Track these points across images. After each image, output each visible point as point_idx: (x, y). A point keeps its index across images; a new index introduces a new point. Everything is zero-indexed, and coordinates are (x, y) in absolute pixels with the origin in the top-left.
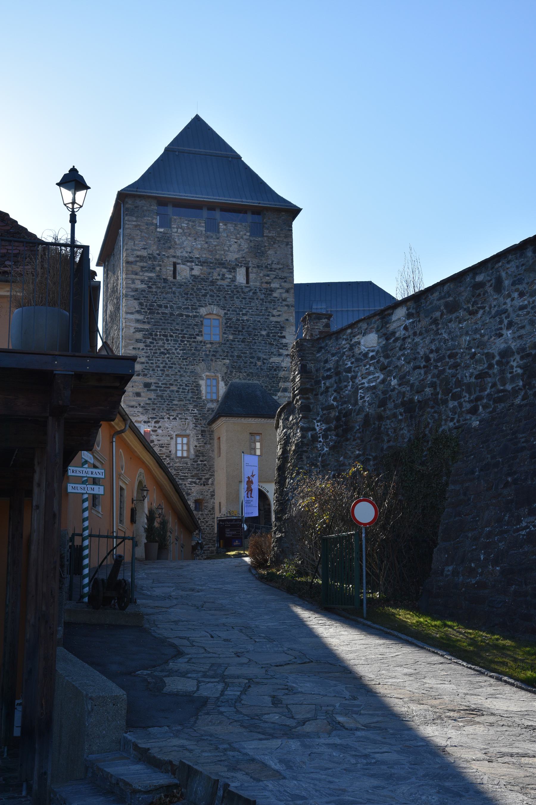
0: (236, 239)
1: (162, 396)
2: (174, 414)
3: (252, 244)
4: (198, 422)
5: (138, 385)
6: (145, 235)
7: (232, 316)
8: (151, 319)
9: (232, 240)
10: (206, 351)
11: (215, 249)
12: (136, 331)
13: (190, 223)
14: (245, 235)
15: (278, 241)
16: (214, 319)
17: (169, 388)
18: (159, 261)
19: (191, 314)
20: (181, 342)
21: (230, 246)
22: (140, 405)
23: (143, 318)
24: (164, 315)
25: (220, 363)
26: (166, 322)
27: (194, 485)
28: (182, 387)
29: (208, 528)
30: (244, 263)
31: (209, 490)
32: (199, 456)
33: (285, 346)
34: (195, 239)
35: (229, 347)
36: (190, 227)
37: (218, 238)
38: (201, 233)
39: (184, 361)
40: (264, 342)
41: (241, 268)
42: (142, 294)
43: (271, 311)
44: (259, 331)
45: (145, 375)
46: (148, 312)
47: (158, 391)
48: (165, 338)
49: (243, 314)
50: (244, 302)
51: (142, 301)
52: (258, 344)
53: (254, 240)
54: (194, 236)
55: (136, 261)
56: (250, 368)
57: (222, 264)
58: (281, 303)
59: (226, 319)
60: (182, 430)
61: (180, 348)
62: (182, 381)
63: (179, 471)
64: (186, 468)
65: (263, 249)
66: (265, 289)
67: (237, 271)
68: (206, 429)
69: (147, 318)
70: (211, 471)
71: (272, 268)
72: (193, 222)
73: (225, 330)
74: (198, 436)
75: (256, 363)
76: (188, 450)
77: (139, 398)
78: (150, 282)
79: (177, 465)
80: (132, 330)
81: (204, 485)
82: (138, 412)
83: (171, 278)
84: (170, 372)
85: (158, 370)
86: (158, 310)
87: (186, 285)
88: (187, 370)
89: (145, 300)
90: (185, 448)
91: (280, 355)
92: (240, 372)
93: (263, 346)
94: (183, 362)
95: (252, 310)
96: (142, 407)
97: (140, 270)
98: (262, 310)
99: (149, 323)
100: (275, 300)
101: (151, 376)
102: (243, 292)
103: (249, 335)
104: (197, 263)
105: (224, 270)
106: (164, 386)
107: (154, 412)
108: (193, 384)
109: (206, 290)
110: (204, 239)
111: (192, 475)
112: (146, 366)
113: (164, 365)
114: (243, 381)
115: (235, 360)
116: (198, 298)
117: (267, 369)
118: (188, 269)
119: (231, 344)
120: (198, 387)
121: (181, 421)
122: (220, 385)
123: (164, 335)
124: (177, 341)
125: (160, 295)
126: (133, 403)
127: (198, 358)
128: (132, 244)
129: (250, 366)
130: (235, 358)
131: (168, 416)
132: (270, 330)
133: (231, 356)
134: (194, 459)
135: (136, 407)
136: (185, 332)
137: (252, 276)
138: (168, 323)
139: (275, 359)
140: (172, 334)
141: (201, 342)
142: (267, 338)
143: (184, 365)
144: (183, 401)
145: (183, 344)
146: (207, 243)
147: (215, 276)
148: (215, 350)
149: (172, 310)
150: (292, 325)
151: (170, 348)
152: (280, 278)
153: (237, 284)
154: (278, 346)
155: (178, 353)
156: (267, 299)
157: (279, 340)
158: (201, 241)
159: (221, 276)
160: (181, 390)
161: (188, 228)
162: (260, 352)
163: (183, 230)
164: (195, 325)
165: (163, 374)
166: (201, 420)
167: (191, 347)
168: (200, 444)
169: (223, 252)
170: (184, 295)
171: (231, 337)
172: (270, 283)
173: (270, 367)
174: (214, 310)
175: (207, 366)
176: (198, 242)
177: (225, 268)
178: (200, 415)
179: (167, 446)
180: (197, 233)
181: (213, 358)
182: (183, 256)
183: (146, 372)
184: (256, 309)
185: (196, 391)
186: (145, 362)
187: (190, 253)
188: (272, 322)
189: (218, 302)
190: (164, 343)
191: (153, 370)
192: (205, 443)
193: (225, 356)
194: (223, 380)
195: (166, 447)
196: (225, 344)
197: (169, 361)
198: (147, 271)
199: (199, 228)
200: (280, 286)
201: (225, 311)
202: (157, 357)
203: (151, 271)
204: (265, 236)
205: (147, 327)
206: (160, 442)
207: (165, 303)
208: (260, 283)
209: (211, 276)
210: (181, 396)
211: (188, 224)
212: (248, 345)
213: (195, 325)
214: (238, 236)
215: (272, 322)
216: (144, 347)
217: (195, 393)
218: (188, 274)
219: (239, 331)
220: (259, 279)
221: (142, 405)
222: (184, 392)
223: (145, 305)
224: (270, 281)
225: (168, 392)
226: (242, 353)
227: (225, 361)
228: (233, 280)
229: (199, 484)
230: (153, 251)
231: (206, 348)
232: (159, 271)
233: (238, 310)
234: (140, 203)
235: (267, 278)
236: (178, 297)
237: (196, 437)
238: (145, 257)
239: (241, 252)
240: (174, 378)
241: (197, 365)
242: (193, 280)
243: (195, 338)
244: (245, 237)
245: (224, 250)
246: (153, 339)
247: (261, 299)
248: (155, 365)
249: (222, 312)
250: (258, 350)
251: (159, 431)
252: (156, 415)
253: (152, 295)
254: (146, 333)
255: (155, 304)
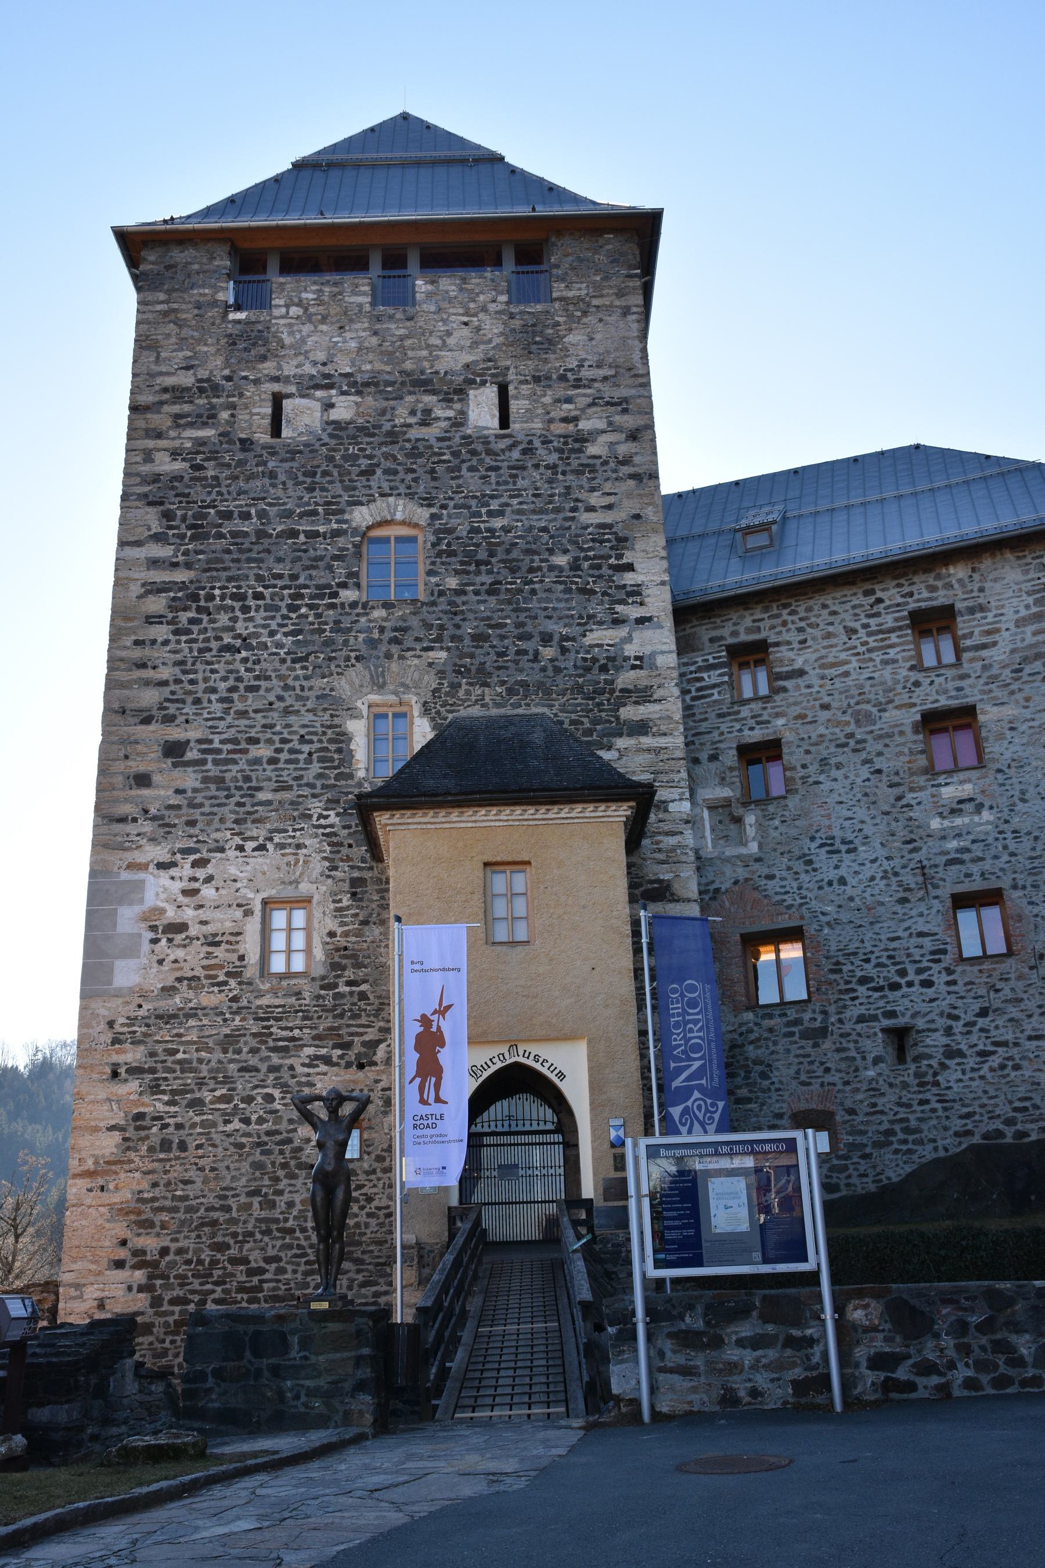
0: (467, 314)
1: (220, 781)
2: (260, 832)
3: (517, 323)
4: (339, 852)
5: (145, 750)
6: (191, 333)
7: (454, 522)
8: (197, 552)
9: (453, 318)
10: (369, 630)
11: (402, 346)
12: (148, 592)
13: (327, 289)
14: (494, 301)
15: (597, 307)
16: (399, 539)
17: (245, 751)
18: (228, 396)
19: (322, 529)
20: (290, 611)
21: (449, 334)
22: (146, 812)
23: (171, 553)
24: (239, 540)
25: (416, 661)
26: (244, 557)
27: (323, 1068)
28: (287, 747)
29: (373, 1222)
30: (493, 375)
31: (377, 1081)
32: (344, 968)
33: (636, 593)
34: (341, 328)
35: (446, 612)
36: (326, 299)
37: (410, 319)
38: (360, 311)
39: (298, 666)
40: (561, 587)
41: (482, 389)
42: (173, 488)
43: (583, 495)
44: (545, 556)
45: (169, 719)
46: (189, 534)
47: (209, 766)
48: (237, 605)
49: (491, 514)
50: (493, 480)
51: (172, 507)
52: (542, 595)
53: (521, 313)
54: (338, 321)
55: (162, 403)
56: (517, 670)
57: (422, 383)
58: (615, 471)
59: (436, 532)
60: (283, 883)
61: (285, 630)
62: (288, 726)
63: (272, 1022)
64: (297, 1011)
65: (550, 331)
66: (560, 436)
67: (471, 397)
68: (367, 875)
69: (186, 553)
70: (384, 1014)
71: (580, 380)
72: (335, 284)
73: (433, 563)
74: (340, 901)
75: (537, 653)
76: (308, 951)
77: (145, 792)
78: (198, 453)
79: (264, 1001)
80: (136, 589)
81: (361, 1066)
82: (138, 835)
83: (263, 437)
84: (252, 702)
85: (210, 701)
86: (220, 526)
87: (311, 451)
88: (306, 693)
89: (180, 502)
90: (299, 941)
91: (618, 622)
92: (482, 685)
93: (559, 600)
94: (294, 669)
95: (520, 499)
96: (154, 819)
97: (169, 424)
98: (552, 495)
99: (188, 566)
100: (594, 465)
101: (187, 721)
102: (489, 452)
103: (513, 571)
104: (345, 388)
105: (429, 399)
106: (230, 747)
107: (192, 831)
108: (324, 733)
109: (370, 457)
110: (366, 325)
111: (314, 1032)
112: (173, 693)
113: (231, 682)
114: (494, 712)
115: (466, 650)
116: (347, 483)
117: (575, 666)
118: (317, 406)
119: (451, 603)
120: (342, 742)
121: (283, 855)
122: (416, 729)
123: (234, 597)
124: (277, 609)
125: (229, 486)
126: (126, 809)
127: (344, 653)
128: (152, 359)
129: (516, 662)
130: (467, 641)
131: (237, 840)
132: (582, 549)
133: (453, 638)
134: (323, 978)
135: (135, 820)
136: (301, 581)
137: (516, 406)
138: (249, 560)
139: (601, 636)
140: (261, 589)
141: (354, 605)
142: (572, 573)
143: (297, 678)
144: (289, 788)
145: (294, 616)
146: (376, 333)
147: (402, 415)
148: (401, 623)
149: (263, 524)
150: (655, 531)
151: (252, 630)
152: (608, 403)
153: (469, 432)
154: (609, 595)
155: (279, 645)
156: (569, 464)
157: (610, 576)
158: (357, 330)
159: (419, 414)
160: (284, 756)
161: (320, 302)
162: (549, 617)
163: (306, 310)
164: (335, 558)
165: (226, 711)
166: (350, 846)
167: (319, 624)
168: (346, 924)
169: (425, 353)
170: (301, 478)
171: (453, 583)
172: (575, 419)
173: (585, 660)
174: (395, 509)
175: (372, 676)
176: (348, 335)
177: (434, 392)
178: (346, 831)
179: (233, 939)
180: (345, 313)
181: (395, 649)
182: (301, 376)
183: (172, 709)
184: (534, 495)
185: (336, 756)
186: (171, 679)
187: (324, 364)
188: (586, 528)
189: (409, 487)
190: (234, 619)
191: (197, 701)
192: (365, 923)
193: (434, 641)
194: (426, 710)
195: (227, 942)
196: (433, 604)
197: (247, 670)
198: (191, 425)
199: (353, 299)
200: (610, 424)
201: (434, 510)
202: (208, 663)
203: (205, 424)
204: (556, 299)
205: (181, 576)
206: (209, 929)
207: (241, 506)
208: (543, 422)
209: (388, 417)
210: (285, 773)
211: (321, 291)
212: (509, 602)
213: (335, 558)
214: (472, 305)
215: (586, 528)
216: (171, 637)
217: (332, 760)
218: (318, 420)
219: (479, 563)
220: (540, 411)
221: (153, 811)
222: (296, 761)
223: (179, 517)
224: (577, 413)
225: (243, 765)
226: (490, 626)
227: (431, 654)
228: (459, 422)
229: (343, 1062)
230: (211, 372)
231: (370, 621)
232: (227, 422)
233: (473, 503)
234: (179, 255)
235: (566, 406)
236: (284, 483)
237: (334, 901)
238: (188, 389)
239: (482, 347)
240: (263, 722)
241: (338, 674)
242: (331, 436)
243: (335, 595)
244: (492, 307)
245: (428, 346)
246: (199, 610)
247: (547, 467)
248: (202, 686)
249: (422, 515)
250: (544, 613)
251: (208, 892)
252: (198, 842)
253: (204, 487)
254: (180, 594)
255: (212, 511)
